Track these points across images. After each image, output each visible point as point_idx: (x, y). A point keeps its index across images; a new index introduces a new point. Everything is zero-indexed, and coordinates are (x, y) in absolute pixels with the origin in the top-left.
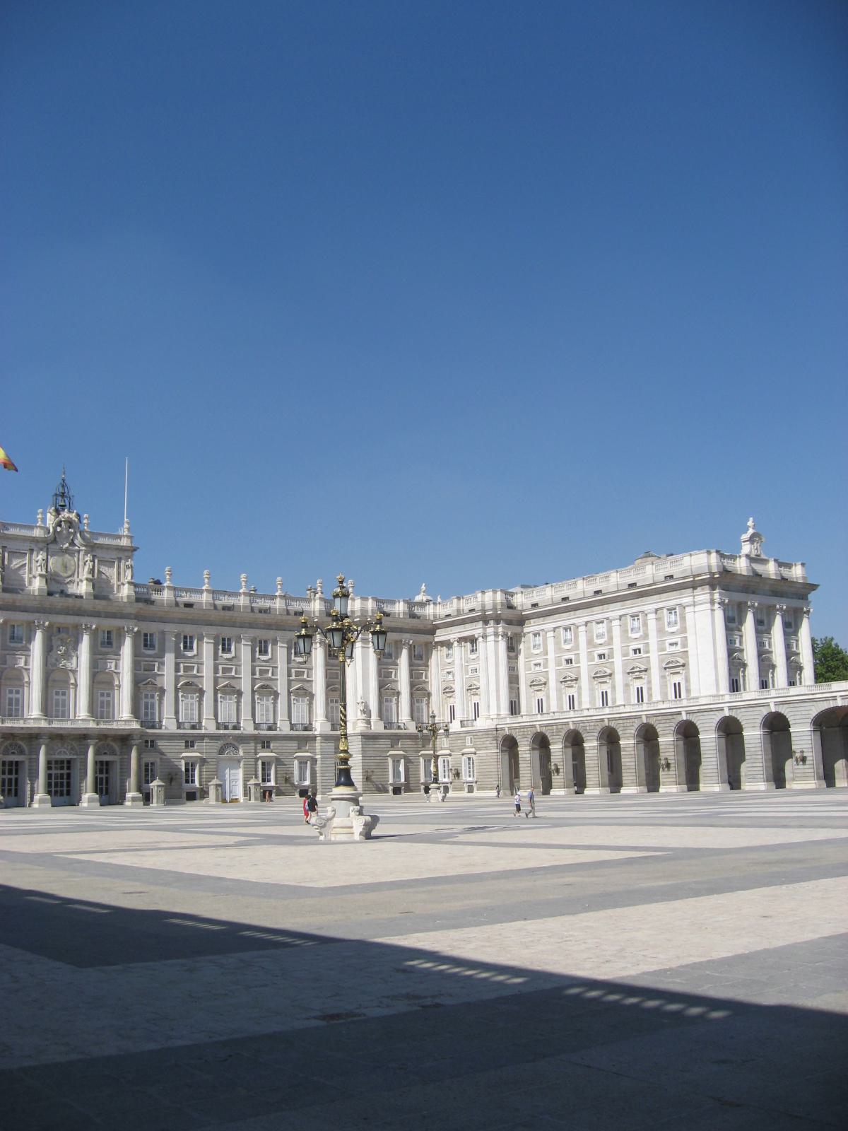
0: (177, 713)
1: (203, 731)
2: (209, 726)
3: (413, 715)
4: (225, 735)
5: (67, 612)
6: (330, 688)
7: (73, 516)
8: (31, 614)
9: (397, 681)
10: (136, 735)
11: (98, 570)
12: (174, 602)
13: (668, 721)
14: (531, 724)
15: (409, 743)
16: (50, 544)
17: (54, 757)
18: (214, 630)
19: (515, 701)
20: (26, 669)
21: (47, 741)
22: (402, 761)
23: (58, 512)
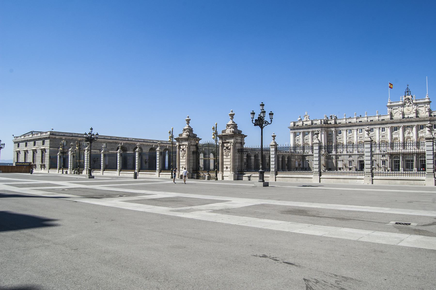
7: (410, 97)
23: (405, 96)
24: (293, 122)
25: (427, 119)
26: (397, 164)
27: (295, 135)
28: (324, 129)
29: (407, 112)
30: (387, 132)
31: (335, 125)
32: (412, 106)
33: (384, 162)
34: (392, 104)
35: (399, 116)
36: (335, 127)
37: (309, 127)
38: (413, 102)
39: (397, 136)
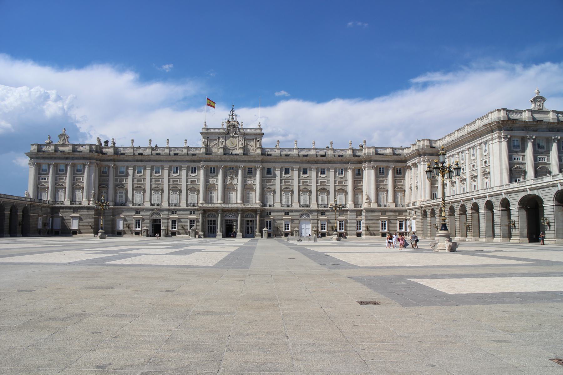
0: (281, 200)
1: (292, 208)
2: (296, 206)
3: (395, 201)
4: (303, 210)
5: (231, 161)
6: (355, 189)
8: (216, 163)
9: (387, 185)
10: (259, 210)
11: (247, 144)
12: (280, 154)
13: (469, 203)
14: (430, 204)
15: (391, 214)
16: (226, 135)
17: (227, 218)
18: (298, 165)
19: (436, 194)
20: (216, 184)
21: (221, 212)
22: (387, 222)
24: (34, 144)
25: (257, 159)
26: (211, 226)
27: (39, 169)
28: (95, 161)
29: (231, 146)
30: (200, 174)
31: (116, 157)
32: (238, 137)
33: (192, 222)
34: (209, 131)
35: (218, 151)
36: (114, 161)
37: (67, 156)
38: (240, 132)
39: (215, 182)
